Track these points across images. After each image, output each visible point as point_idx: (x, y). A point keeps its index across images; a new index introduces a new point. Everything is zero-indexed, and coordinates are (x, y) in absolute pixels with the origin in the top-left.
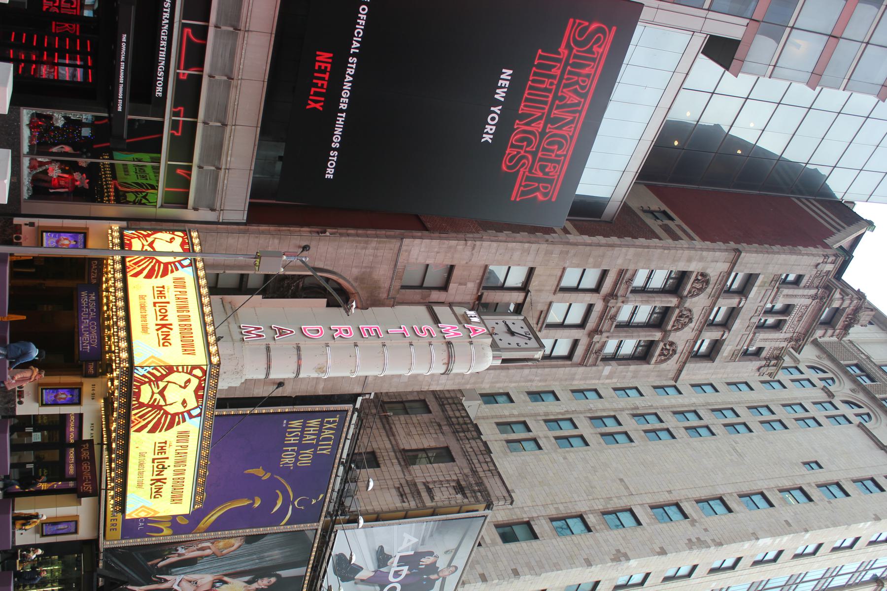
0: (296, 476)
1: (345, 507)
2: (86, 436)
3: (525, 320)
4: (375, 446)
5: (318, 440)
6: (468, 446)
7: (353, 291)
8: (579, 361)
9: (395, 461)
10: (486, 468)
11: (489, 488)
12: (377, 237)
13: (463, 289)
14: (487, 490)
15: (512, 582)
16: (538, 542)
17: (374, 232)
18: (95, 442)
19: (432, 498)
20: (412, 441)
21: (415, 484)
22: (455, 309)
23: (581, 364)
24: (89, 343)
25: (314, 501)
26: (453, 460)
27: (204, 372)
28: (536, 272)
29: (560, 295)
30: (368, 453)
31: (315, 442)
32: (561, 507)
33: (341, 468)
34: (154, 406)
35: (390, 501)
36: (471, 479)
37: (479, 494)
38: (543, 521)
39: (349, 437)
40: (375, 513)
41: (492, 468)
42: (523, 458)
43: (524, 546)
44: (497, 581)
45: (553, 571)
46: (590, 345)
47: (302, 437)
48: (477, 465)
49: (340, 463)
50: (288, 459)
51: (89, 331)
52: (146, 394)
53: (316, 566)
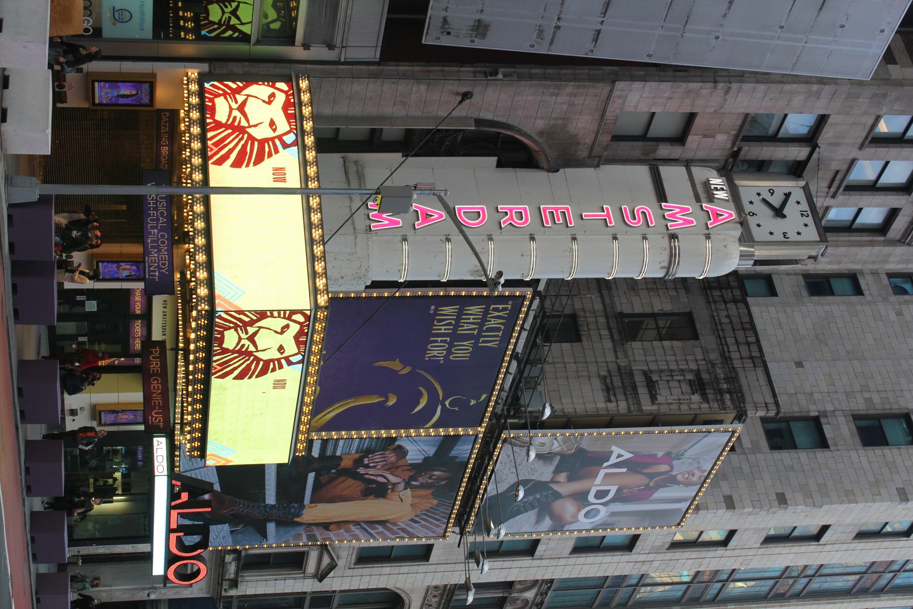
0: (447, 371)
2: (157, 336)
3: (806, 189)
4: (578, 305)
5: (480, 330)
7: (537, 148)
8: (898, 237)
9: (605, 332)
10: (745, 353)
14: (741, 391)
15: (775, 513)
16: (827, 453)
17: (571, 71)
18: (168, 346)
19: (653, 398)
20: (636, 300)
21: (631, 374)
22: (695, 170)
24: (158, 267)
25: (473, 402)
26: (696, 337)
27: (307, 318)
28: (830, 120)
30: (566, 316)
31: (476, 332)
32: (876, 399)
33: (514, 364)
34: (242, 352)
35: (588, 397)
36: (719, 371)
37: (727, 396)
38: (842, 420)
39: (527, 326)
40: (564, 416)
41: (756, 354)
42: (827, 308)
43: (802, 458)
44: (750, 509)
45: (842, 502)
47: (457, 326)
48: (733, 348)
49: (514, 356)
50: (436, 351)
51: (157, 247)
52: (231, 339)
53: (476, 478)
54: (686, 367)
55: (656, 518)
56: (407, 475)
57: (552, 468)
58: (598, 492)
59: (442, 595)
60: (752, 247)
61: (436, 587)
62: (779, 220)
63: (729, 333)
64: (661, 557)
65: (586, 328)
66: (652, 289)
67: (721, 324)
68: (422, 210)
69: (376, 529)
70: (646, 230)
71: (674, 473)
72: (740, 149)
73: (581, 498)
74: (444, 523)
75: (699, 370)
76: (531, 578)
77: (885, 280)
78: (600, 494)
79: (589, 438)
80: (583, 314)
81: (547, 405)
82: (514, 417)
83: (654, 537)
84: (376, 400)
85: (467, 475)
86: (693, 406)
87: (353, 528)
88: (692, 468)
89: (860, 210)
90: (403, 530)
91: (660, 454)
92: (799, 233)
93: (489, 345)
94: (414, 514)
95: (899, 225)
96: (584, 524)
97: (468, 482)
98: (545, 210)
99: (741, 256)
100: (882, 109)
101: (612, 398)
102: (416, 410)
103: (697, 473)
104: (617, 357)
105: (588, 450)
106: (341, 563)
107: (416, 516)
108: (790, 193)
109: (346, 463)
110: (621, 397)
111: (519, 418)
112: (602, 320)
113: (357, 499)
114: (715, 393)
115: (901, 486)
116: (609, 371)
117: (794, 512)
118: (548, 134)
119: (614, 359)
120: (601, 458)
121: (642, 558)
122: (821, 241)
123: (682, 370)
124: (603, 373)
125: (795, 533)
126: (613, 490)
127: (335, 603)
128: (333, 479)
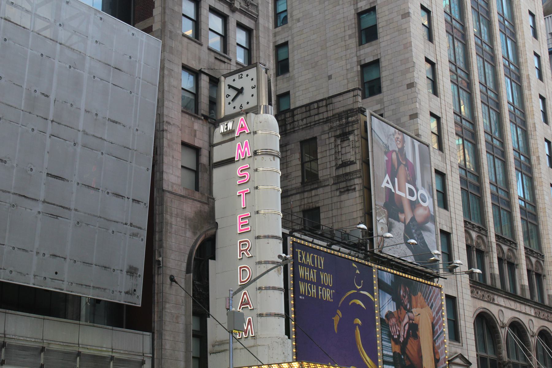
0: (340, 287)
1: (359, 243)
3: (226, 76)
4: (297, 209)
5: (314, 268)
6: (301, 123)
7: (204, 236)
8: (253, 22)
9: (313, 193)
11: (344, 109)
12: (162, 213)
13: (198, 132)
14: (347, 111)
16: (382, 60)
19: (352, 163)
20: (294, 175)
21: (338, 177)
22: (215, 141)
23: (255, 19)
25: (358, 272)
26: (315, 138)
28: (185, 63)
29: (203, 39)
30: (304, 216)
31: (315, 271)
32: (349, 32)
33: (334, 247)
35: (353, 202)
36: (335, 124)
37: (350, 119)
38: (362, 52)
39: (311, 239)
40: (365, 216)
41: (324, 103)
42: (296, 62)
43: (385, 74)
44: (417, 104)
46: (241, 11)
47: (311, 282)
48: (321, 116)
49: (329, 247)
50: (327, 295)
53: (404, 269)
54: (333, 144)
55: (425, 159)
56: (403, 311)
57: (396, 223)
58: (410, 195)
59: (476, 288)
60: (260, 107)
61: (472, 292)
62: (245, 91)
63: (312, 119)
64: (448, 156)
65: (311, 204)
66: (287, 165)
67: (307, 124)
68: (242, 304)
69: (437, 329)
70: (252, 169)
72: (203, 115)
73: (414, 205)
74: (432, 288)
75: (335, 136)
76: (464, 234)
77: (277, 29)
78: (411, 193)
79: (378, 201)
80: (302, 207)
81: (358, 226)
82: (366, 247)
83: (436, 161)
84: (358, 331)
85: (401, 274)
86: (356, 139)
87: (437, 344)
88: (394, 139)
89: (238, 44)
90: (437, 313)
91: (386, 158)
92: (252, 79)
93: (322, 262)
94: (428, 307)
95: (246, 21)
96: (429, 203)
97: (405, 273)
98: (240, 230)
99: (266, 113)
100: (179, 33)
101: (353, 187)
102: (363, 306)
104: (328, 185)
105: (384, 201)
106: (459, 351)
107: (428, 305)
108: (228, 85)
109: (397, 349)
110: (352, 182)
111: (366, 244)
112: (306, 195)
113: (419, 342)
114: (349, 126)
115: (400, 17)
116: (337, 190)
118: (194, 229)
119: (330, 187)
120: (390, 194)
121: (449, 167)
122: (256, 66)
123: (335, 146)
124: (338, 193)
125: (431, 77)
126: (408, 186)
127: (484, 354)
128: (408, 357)
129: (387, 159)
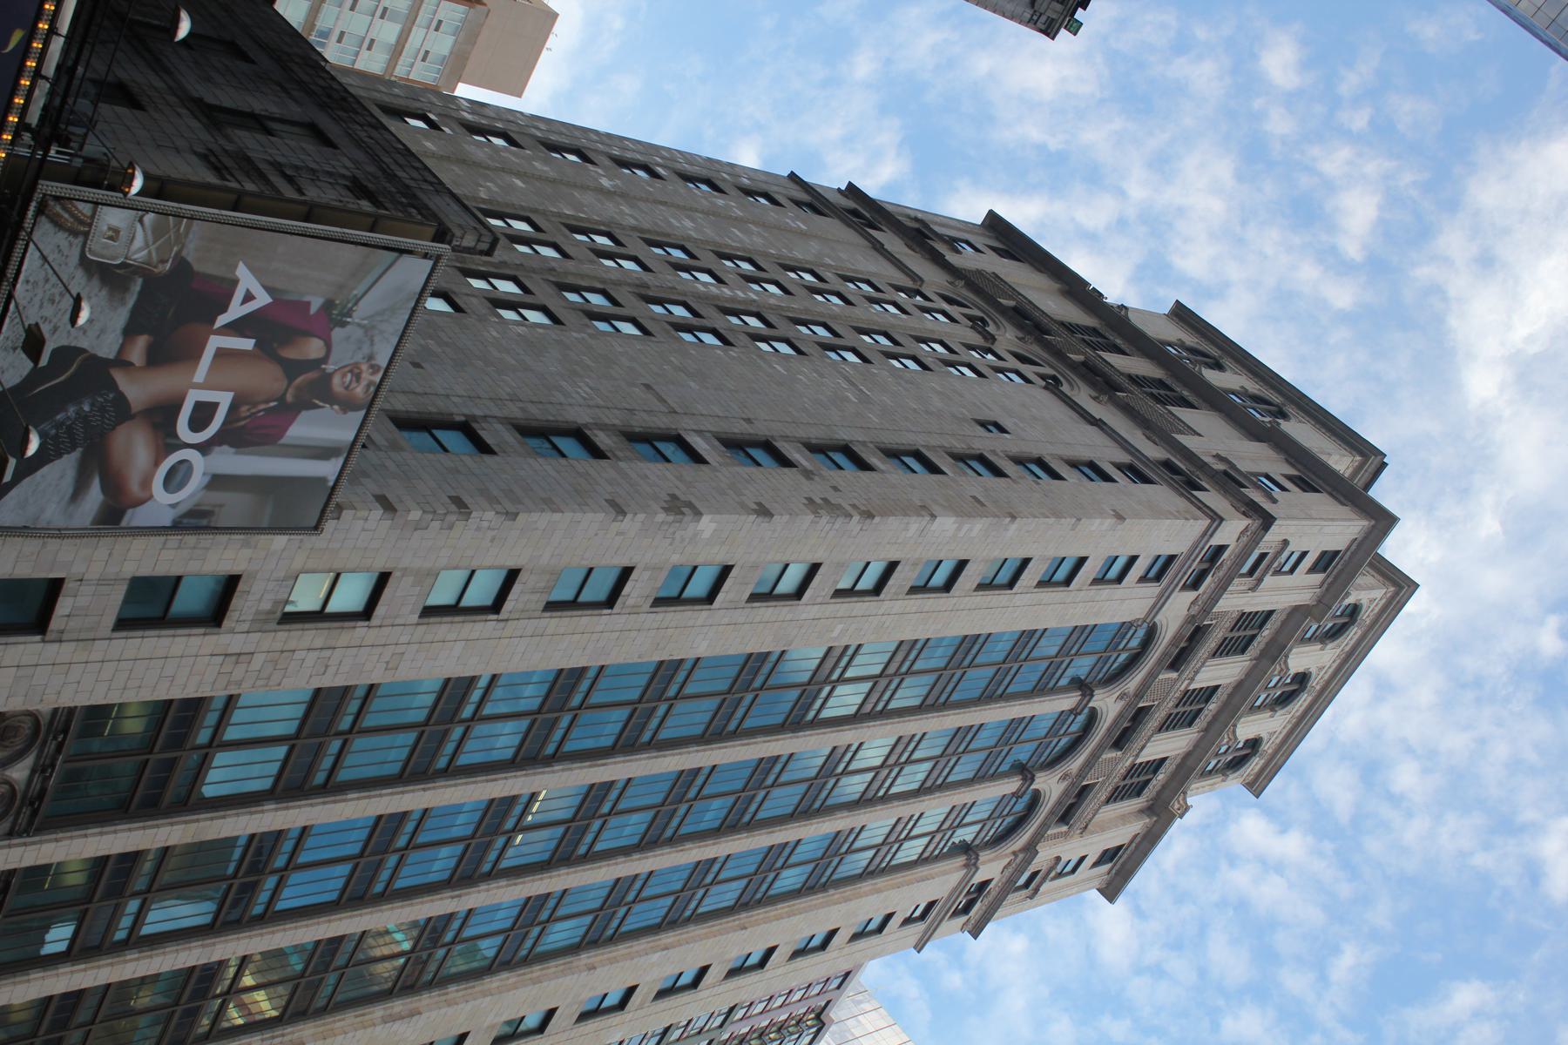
15: (451, 527)
71: (330, 368)
88: (358, 357)
103: (367, 376)
105: (197, 267)
117: (478, 529)
126: (224, 399)
129: (313, 309)
